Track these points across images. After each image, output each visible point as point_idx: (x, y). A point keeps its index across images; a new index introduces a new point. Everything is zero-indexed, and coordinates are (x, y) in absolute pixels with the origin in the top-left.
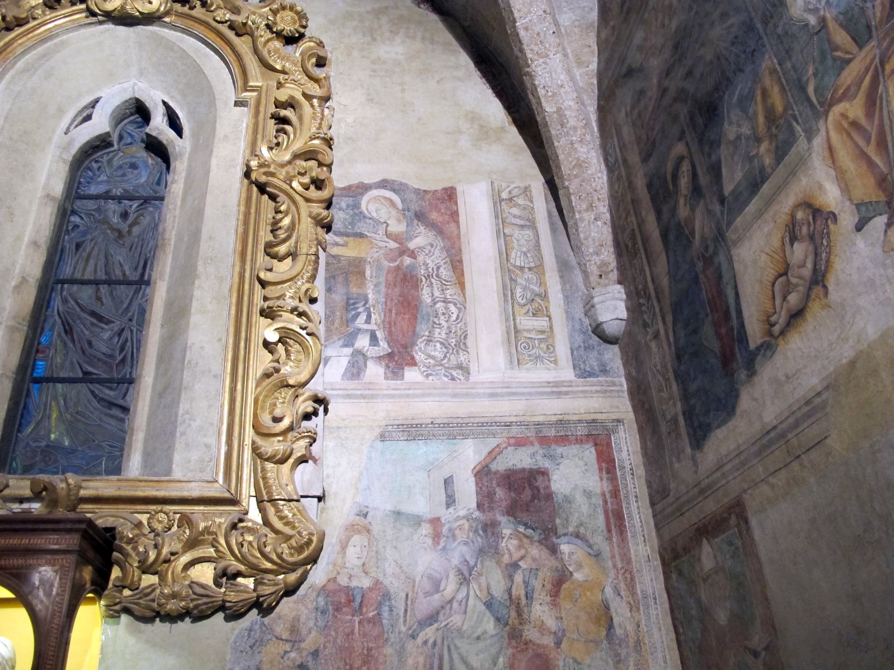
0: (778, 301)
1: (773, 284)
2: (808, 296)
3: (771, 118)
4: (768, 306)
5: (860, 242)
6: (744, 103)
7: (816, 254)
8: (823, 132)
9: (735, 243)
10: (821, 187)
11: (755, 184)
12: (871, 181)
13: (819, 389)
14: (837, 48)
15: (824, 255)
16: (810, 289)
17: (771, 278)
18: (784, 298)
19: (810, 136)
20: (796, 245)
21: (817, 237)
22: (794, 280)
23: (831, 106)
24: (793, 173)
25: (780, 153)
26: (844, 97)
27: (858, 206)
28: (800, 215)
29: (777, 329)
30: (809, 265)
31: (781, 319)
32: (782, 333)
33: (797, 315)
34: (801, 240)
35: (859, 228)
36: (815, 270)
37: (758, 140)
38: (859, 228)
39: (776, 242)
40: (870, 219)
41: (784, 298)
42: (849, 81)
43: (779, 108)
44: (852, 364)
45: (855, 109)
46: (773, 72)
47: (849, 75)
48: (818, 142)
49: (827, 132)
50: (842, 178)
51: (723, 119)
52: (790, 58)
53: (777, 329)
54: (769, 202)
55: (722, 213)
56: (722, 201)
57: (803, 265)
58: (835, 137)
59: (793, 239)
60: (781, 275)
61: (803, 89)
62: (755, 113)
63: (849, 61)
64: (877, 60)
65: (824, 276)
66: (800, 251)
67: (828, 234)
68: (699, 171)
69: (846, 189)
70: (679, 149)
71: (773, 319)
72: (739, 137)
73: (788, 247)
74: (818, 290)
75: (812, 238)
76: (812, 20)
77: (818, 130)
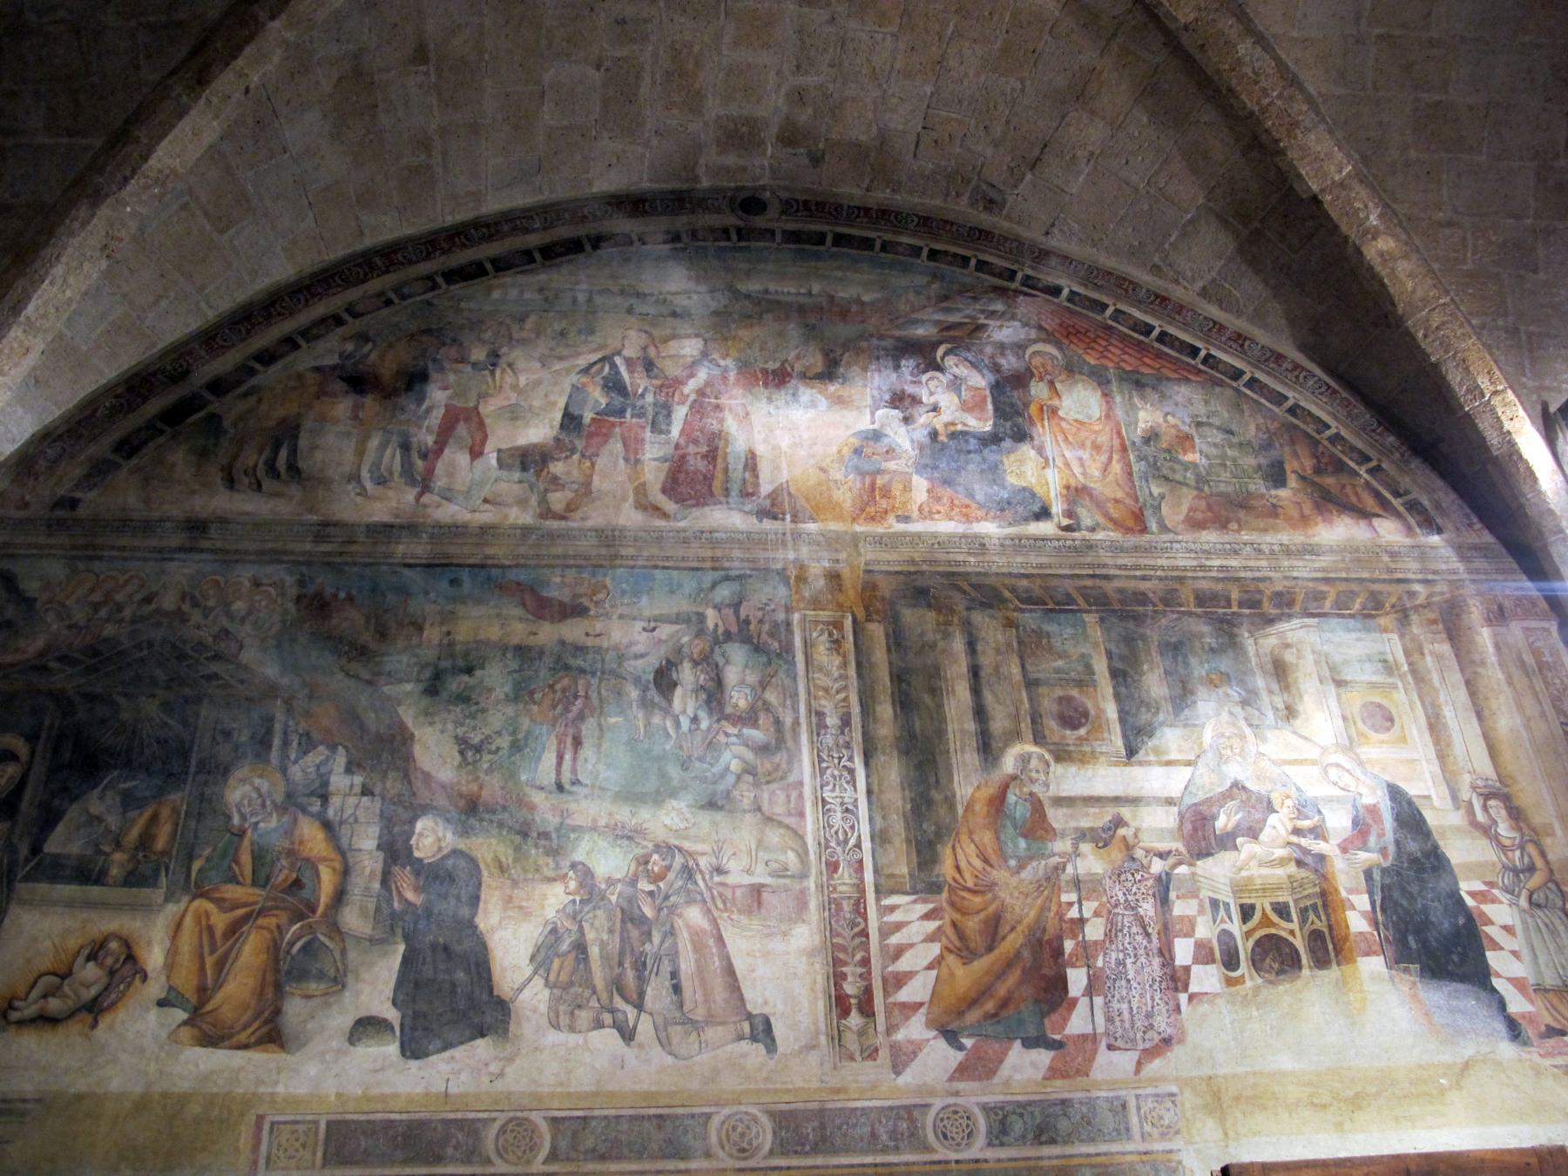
0: (34, 994)
1: (41, 976)
2: (71, 1015)
3: (146, 840)
4: (21, 989)
5: (153, 1014)
6: (129, 801)
7: (106, 989)
8: (183, 905)
9: (23, 903)
10: (149, 943)
11: (87, 873)
12: (194, 982)
13: (30, 1096)
14: (237, 863)
15: (113, 996)
16: (79, 1010)
17: (43, 968)
18: (45, 996)
19: (169, 897)
20: (91, 965)
21: (117, 977)
22: (66, 989)
23: (202, 895)
24: (133, 907)
25: (134, 879)
26: (219, 902)
27: (171, 988)
28: (114, 945)
29: (15, 1016)
30: (93, 991)
31: (30, 1011)
32: (21, 1023)
33: (47, 1021)
34: (101, 965)
35: (161, 1003)
36: (95, 1000)
37: (118, 845)
38: (161, 1003)
39: (73, 943)
40: (173, 1006)
41: (45, 996)
42: (228, 896)
43: (160, 844)
44: (79, 1097)
45: (220, 920)
46: (175, 811)
47: (232, 892)
48: (172, 909)
49: (186, 910)
50: (172, 954)
51: (94, 787)
52: (198, 821)
53: (15, 1016)
54: (89, 905)
55: (27, 860)
56: (36, 850)
57: (88, 987)
58: (188, 921)
59: (92, 957)
60: (54, 974)
61: (191, 857)
62: (133, 821)
63: (238, 883)
64: (257, 907)
65: (102, 1011)
66: (91, 972)
67: (129, 985)
68: (28, 793)
69: (170, 966)
70: (20, 746)
71: (17, 1004)
72: (99, 819)
73: (81, 960)
74: (89, 1018)
75: (112, 973)
76: (236, 820)
77: (178, 901)
